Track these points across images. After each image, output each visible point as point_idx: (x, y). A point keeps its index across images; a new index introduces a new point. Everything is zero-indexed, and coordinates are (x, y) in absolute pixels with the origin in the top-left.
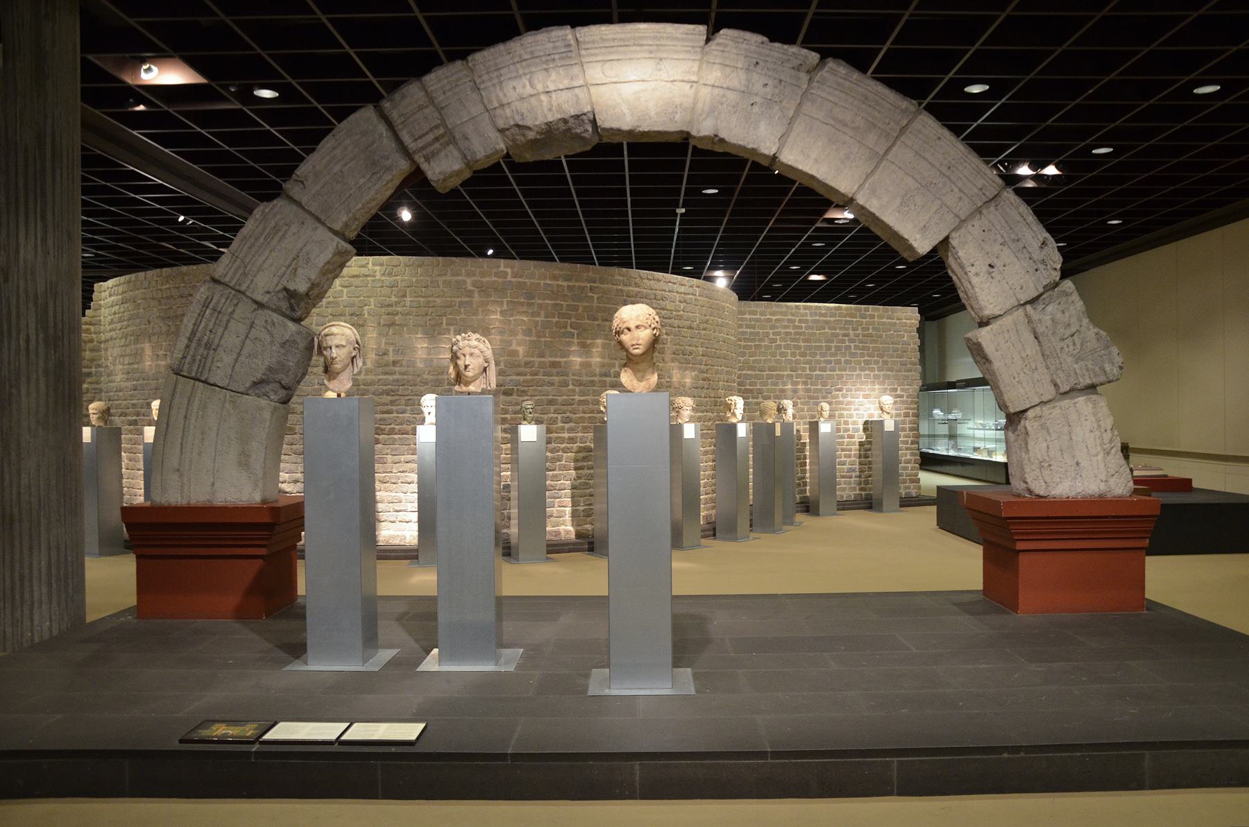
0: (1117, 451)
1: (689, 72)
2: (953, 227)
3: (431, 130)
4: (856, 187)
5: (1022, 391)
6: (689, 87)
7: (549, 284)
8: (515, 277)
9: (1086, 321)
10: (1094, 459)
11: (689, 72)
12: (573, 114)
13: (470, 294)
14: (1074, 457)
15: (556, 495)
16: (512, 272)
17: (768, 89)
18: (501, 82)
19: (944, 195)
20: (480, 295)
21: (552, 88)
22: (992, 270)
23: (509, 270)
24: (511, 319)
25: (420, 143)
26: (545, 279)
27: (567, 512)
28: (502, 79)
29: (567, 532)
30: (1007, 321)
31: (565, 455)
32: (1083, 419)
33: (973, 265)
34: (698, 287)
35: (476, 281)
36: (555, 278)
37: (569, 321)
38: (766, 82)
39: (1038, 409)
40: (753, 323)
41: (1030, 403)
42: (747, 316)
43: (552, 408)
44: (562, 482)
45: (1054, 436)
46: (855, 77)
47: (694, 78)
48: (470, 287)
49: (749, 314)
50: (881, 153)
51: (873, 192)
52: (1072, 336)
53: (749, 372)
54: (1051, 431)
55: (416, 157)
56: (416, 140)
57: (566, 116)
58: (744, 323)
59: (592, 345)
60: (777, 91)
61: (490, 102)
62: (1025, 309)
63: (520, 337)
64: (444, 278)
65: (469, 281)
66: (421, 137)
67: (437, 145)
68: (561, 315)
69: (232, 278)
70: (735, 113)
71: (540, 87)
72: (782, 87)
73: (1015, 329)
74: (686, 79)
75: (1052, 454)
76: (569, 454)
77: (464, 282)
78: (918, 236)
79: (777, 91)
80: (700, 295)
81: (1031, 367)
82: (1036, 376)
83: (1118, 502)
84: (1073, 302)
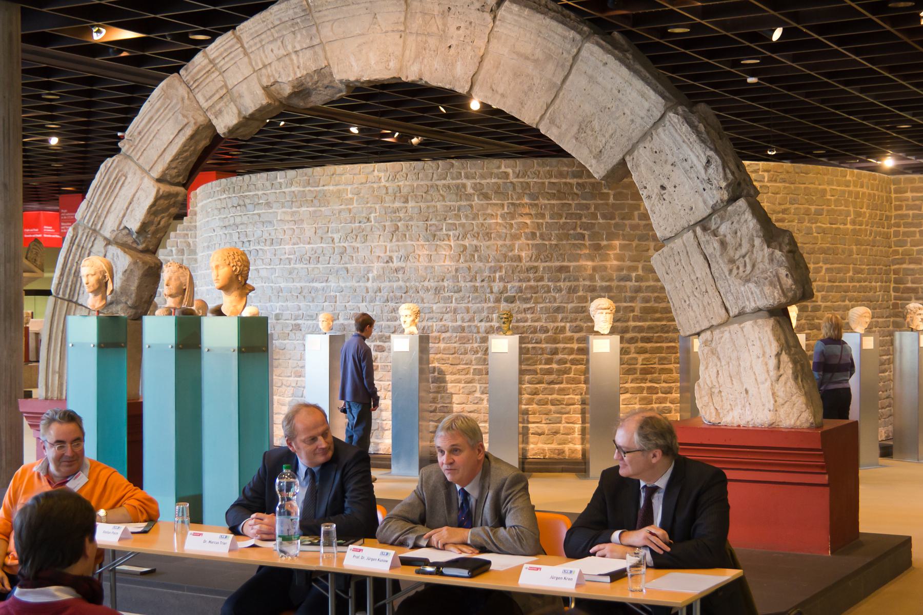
0: (788, 379)
1: (398, 23)
2: (627, 150)
3: (217, 91)
4: (538, 118)
5: (692, 313)
6: (399, 36)
7: (553, 183)
8: (518, 177)
9: (757, 242)
10: (761, 386)
11: (398, 23)
12: (314, 69)
13: (469, 197)
14: (742, 383)
15: (563, 410)
16: (514, 172)
17: (461, 32)
18: (263, 46)
19: (618, 118)
20: (478, 199)
21: (298, 48)
22: (663, 192)
23: (510, 171)
24: (513, 222)
25: (210, 103)
26: (551, 177)
27: (576, 430)
28: (263, 43)
29: (573, 451)
30: (677, 244)
31: (574, 367)
32: (749, 344)
33: (645, 188)
34: (764, 171)
35: (475, 184)
36: (561, 175)
37: (579, 222)
38: (459, 25)
39: (709, 333)
40: (917, 202)
41: (700, 326)
42: (909, 195)
43: (560, 316)
44: (571, 396)
45: (724, 363)
46: (526, 13)
47: (402, 28)
48: (470, 190)
49: (912, 191)
50: (559, 83)
51: (552, 122)
52: (744, 257)
53: (912, 266)
54: (721, 356)
55: (209, 114)
56: (207, 100)
57: (309, 72)
58: (904, 203)
59: (610, 247)
60: (468, 32)
61: (257, 64)
62: (694, 232)
63: (523, 240)
64: (443, 182)
65: (469, 183)
66: (211, 97)
67: (221, 104)
68: (569, 216)
69: (89, 221)
70: (436, 56)
71: (290, 48)
72: (472, 29)
73: (685, 251)
74: (395, 29)
75: (721, 380)
76: (579, 367)
77: (464, 186)
78: (594, 162)
79: (468, 32)
80: (769, 181)
81: (701, 291)
82: (706, 299)
83: (793, 433)
84: (746, 221)
